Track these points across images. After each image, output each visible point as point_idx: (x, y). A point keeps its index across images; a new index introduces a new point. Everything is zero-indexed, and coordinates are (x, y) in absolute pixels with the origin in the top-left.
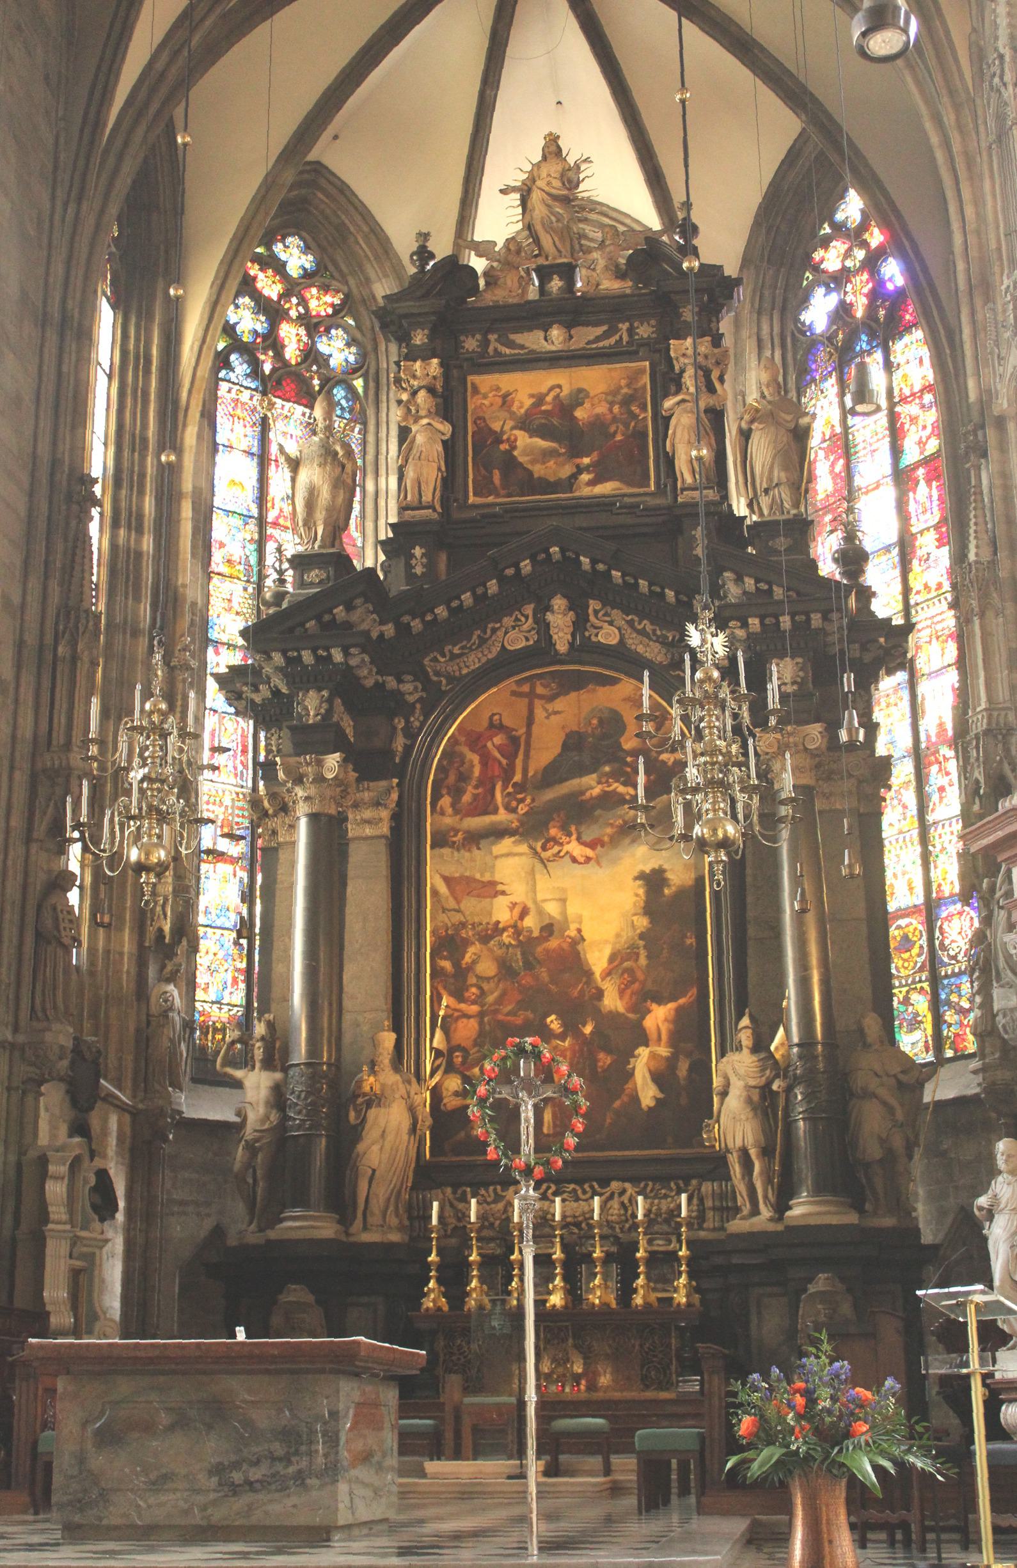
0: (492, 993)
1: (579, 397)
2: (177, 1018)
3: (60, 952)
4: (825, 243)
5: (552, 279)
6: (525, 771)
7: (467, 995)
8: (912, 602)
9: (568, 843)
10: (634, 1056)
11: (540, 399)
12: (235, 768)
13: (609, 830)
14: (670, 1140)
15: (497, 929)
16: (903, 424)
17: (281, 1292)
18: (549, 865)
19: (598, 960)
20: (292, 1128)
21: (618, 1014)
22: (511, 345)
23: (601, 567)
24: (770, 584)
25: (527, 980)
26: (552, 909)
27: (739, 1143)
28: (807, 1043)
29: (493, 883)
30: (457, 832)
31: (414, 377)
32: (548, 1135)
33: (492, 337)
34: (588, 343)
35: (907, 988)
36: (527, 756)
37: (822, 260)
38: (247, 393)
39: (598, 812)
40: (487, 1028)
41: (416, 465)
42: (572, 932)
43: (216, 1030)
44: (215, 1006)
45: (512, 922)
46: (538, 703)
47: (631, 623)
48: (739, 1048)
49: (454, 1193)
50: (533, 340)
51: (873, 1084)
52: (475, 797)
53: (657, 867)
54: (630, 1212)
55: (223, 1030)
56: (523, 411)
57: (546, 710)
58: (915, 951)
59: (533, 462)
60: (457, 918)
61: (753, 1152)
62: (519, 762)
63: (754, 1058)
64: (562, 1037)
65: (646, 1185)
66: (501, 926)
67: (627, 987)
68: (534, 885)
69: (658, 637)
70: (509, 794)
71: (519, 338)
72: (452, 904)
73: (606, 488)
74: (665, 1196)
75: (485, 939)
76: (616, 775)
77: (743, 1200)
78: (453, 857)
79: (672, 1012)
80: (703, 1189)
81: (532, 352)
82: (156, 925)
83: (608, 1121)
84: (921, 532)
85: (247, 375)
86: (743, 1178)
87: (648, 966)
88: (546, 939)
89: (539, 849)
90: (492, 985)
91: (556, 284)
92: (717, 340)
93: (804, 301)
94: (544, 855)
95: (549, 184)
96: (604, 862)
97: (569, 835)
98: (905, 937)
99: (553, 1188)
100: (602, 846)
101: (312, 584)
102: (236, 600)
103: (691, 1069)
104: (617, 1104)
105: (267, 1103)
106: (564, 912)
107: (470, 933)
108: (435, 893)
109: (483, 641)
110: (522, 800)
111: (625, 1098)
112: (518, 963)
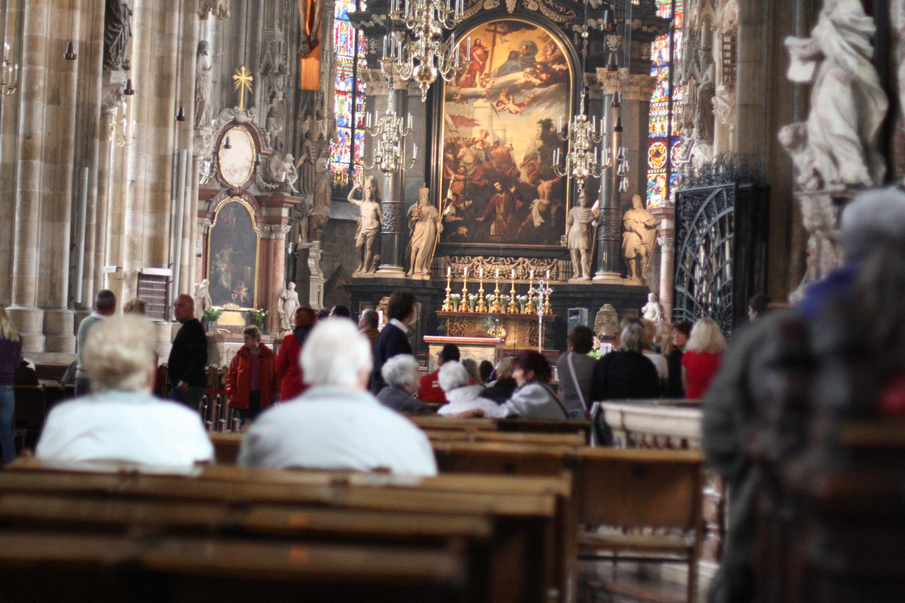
0: (471, 170)
2: (328, 175)
3: (310, 165)
7: (459, 171)
9: (509, 104)
10: (532, 203)
12: (347, 47)
13: (527, 99)
14: (546, 241)
15: (474, 142)
17: (380, 300)
18: (499, 113)
19: (519, 159)
24: (609, 3)
25: (487, 166)
26: (499, 134)
27: (576, 247)
28: (607, 209)
29: (473, 120)
30: (457, 94)
32: (493, 236)
35: (656, 175)
39: (523, 90)
40: (468, 186)
42: (508, 145)
43: (337, 175)
45: (481, 139)
46: (498, 36)
48: (579, 205)
49: (451, 258)
51: (634, 226)
52: (467, 79)
53: (548, 118)
54: (526, 271)
55: (340, 175)
57: (501, 39)
58: (661, 158)
60: (456, 135)
61: (582, 251)
63: (586, 210)
64: (501, 192)
65: (534, 260)
66: (476, 140)
67: (532, 171)
68: (492, 122)
69: (556, 9)
70: (482, 79)
72: (454, 128)
74: (542, 265)
75: (468, 146)
76: (532, 73)
77: (576, 269)
78: (455, 106)
79: (550, 185)
80: (559, 263)
82: (319, 131)
83: (519, 231)
86: (577, 261)
87: (541, 163)
88: (496, 148)
89: (495, 105)
90: (471, 166)
94: (497, 108)
96: (524, 114)
99: (494, 259)
100: (524, 106)
103: (557, 211)
104: (523, 224)
105: (372, 217)
106: (505, 136)
107: (462, 142)
108: (446, 123)
110: (487, 82)
111: (527, 221)
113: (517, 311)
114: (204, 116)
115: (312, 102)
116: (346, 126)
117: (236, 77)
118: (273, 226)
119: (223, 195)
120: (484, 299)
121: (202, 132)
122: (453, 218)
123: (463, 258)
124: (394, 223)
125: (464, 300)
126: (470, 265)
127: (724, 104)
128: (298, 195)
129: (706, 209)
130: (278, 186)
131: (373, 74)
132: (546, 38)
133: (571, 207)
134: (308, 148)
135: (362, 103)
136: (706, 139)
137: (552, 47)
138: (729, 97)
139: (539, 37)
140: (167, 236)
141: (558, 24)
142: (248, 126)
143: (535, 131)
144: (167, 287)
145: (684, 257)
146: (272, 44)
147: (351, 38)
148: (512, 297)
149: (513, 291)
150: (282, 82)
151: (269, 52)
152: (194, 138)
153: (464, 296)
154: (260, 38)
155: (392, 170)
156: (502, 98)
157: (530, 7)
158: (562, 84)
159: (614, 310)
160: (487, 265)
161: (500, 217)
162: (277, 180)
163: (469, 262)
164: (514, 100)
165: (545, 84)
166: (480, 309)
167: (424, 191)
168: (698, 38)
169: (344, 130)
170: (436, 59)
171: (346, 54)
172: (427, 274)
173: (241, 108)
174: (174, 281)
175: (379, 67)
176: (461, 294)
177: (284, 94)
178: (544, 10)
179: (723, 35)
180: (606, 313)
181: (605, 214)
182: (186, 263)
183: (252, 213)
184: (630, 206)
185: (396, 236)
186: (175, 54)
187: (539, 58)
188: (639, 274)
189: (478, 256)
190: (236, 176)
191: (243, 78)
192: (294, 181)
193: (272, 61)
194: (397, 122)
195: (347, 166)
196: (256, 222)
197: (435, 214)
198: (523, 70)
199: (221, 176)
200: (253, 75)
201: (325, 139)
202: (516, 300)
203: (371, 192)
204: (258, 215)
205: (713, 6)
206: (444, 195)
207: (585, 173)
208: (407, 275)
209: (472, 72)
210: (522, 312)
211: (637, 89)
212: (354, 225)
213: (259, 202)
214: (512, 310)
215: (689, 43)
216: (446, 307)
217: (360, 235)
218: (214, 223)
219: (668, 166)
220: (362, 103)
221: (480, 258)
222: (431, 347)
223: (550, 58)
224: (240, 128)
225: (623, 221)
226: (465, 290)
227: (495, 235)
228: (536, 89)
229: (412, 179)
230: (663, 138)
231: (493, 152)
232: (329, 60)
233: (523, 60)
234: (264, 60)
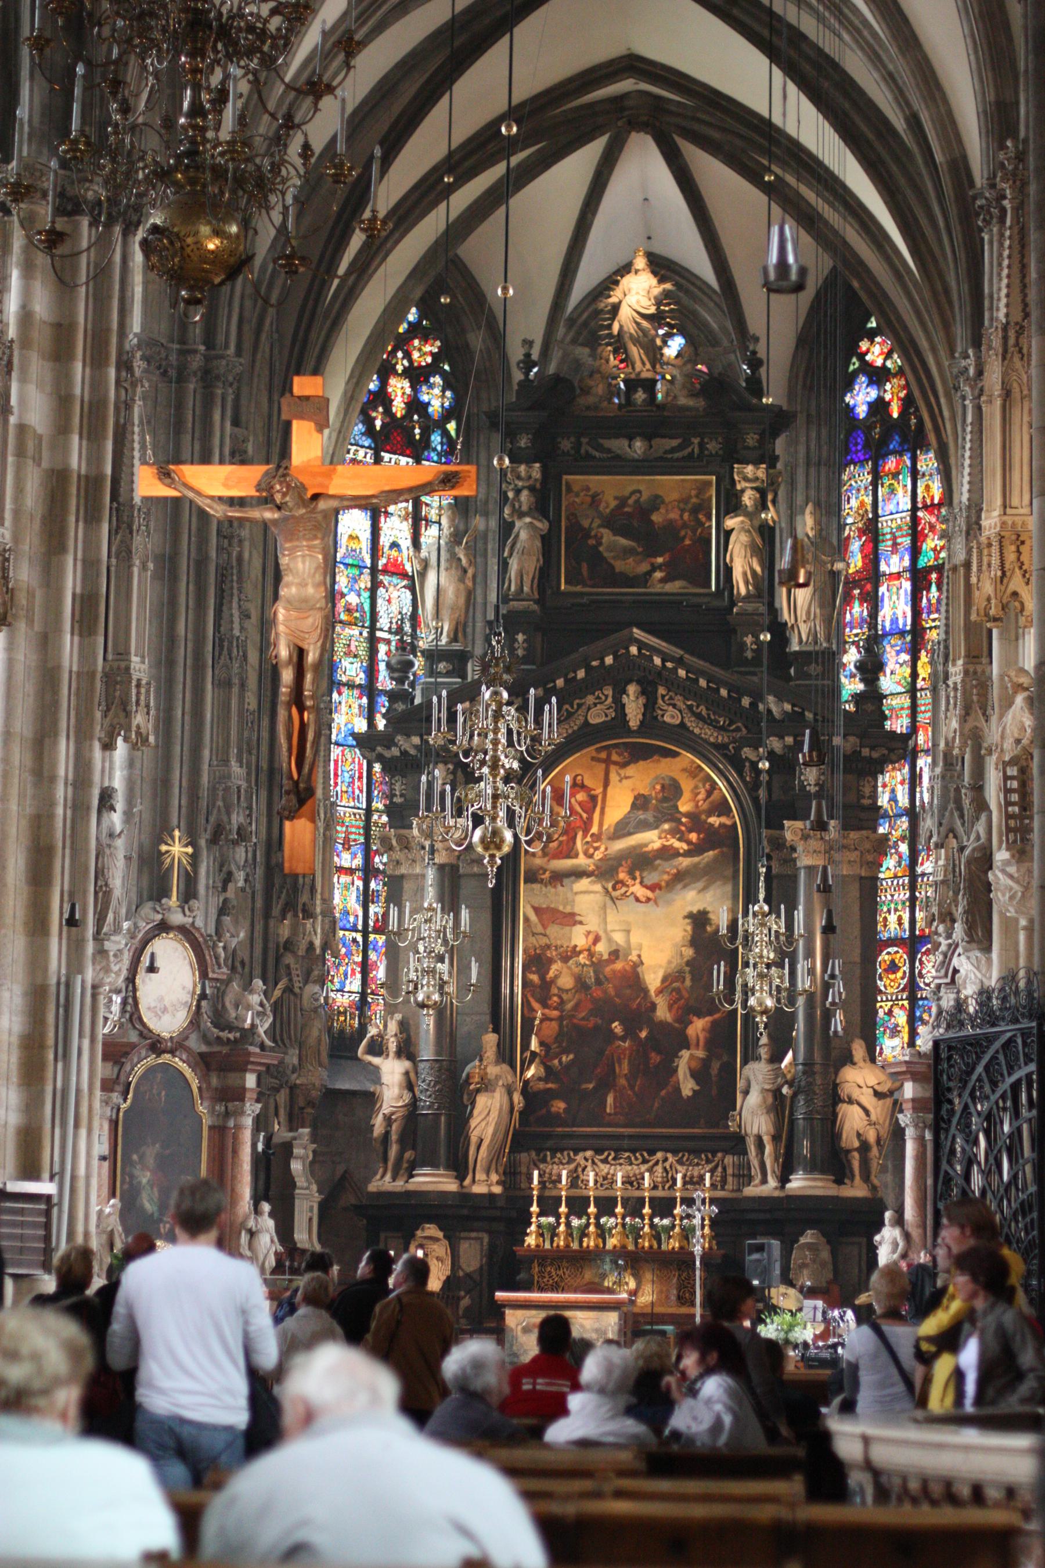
1: (656, 502)
3: (292, 997)
4: (871, 335)
5: (636, 391)
6: (601, 825)
8: (919, 686)
11: (623, 501)
13: (666, 877)
14: (702, 1121)
15: (575, 952)
16: (923, 529)
19: (653, 980)
20: (423, 1108)
21: (669, 1024)
22: (600, 448)
23: (669, 665)
25: (598, 993)
26: (619, 938)
27: (755, 1131)
28: (808, 1064)
29: (573, 915)
30: (545, 871)
31: (519, 478)
33: (584, 440)
34: (666, 452)
36: (602, 813)
37: (868, 351)
38: (362, 452)
39: (658, 862)
41: (520, 559)
42: (635, 958)
43: (339, 1013)
44: (339, 994)
46: (613, 769)
47: (690, 707)
48: (758, 1058)
49: (538, 1155)
50: (619, 445)
51: (856, 1094)
55: (345, 1012)
56: (608, 511)
58: (900, 974)
59: (614, 558)
60: (544, 941)
61: (766, 1139)
62: (596, 816)
63: (770, 1067)
64: (623, 1039)
67: (675, 1002)
68: (605, 919)
71: (607, 443)
72: (539, 929)
73: (675, 587)
74: (698, 1164)
75: (565, 959)
76: (673, 832)
77: (756, 1171)
80: (726, 1161)
81: (618, 457)
84: (931, 628)
85: (363, 434)
91: (640, 396)
92: (771, 461)
93: (849, 385)
94: (615, 894)
95: (638, 302)
96: (660, 902)
97: (634, 879)
98: (893, 961)
99: (613, 1154)
100: (660, 889)
101: (440, 674)
102: (354, 644)
103: (722, 1068)
104: (663, 1093)
105: (400, 1085)
106: (628, 941)
108: (527, 920)
109: (570, 715)
110: (597, 849)
111: (670, 1088)
112: (591, 980)
113: (655, 1246)
114: (110, 916)
115: (295, 889)
116: (357, 931)
117: (164, 848)
118: (230, 1105)
119: (143, 1053)
120: (598, 1225)
121: (107, 945)
122: (541, 1085)
123: (559, 1155)
124: (439, 1095)
125: (562, 1228)
126: (572, 1166)
127: (1010, 882)
128: (272, 1049)
129: (987, 1068)
130: (238, 1035)
131: (400, 838)
132: (694, 772)
133: (745, 1062)
134: (288, 967)
135: (380, 888)
136: (979, 942)
137: (707, 786)
138: (1018, 871)
139: (684, 770)
140: (48, 1126)
141: (717, 746)
142: (186, 933)
143: (679, 932)
144: (48, 1213)
145: (953, 1152)
146: (227, 789)
147: (360, 778)
148: (646, 1221)
149: (647, 1210)
150: (243, 855)
151: (220, 803)
152: (94, 955)
153: (563, 1220)
154: (205, 779)
155: (436, 1003)
156: (622, 876)
157: (667, 719)
158: (725, 849)
159: (823, 1240)
160: (602, 1166)
161: (623, 1082)
162: (236, 1023)
163: (570, 1161)
164: (642, 878)
165: (695, 850)
166: (590, 1242)
167: (490, 1039)
168: (958, 768)
169: (350, 935)
170: (511, 815)
171: (352, 804)
172: (498, 1183)
173: (173, 901)
174: (60, 1204)
175: (410, 827)
176: (558, 1217)
177: (247, 875)
178: (691, 723)
179: (1006, 764)
180: (809, 1246)
181: (804, 1073)
182: (82, 1171)
183: (195, 1083)
184: (848, 1059)
185: (443, 1119)
186: (60, 811)
187: (684, 806)
188: (866, 1177)
189: (585, 1150)
190: (166, 1018)
191: (177, 849)
192: (267, 1025)
193: (225, 818)
194: (442, 920)
195: (356, 997)
196: (201, 1098)
197: (510, 1079)
198: (656, 828)
199: (140, 1019)
200: (192, 843)
201: (318, 951)
202: (652, 1226)
203: (399, 1042)
204: (204, 1086)
205: (984, 714)
206: (526, 1044)
207: (770, 1003)
208: (461, 1186)
209: (570, 833)
210: (664, 1247)
211: (854, 856)
212: (371, 1099)
213: (204, 1063)
214: (647, 1244)
215: (943, 777)
216: (531, 1241)
217: (380, 1117)
218: (129, 1101)
219: (912, 987)
220: (380, 888)
221: (589, 1153)
222: (508, 1312)
223: (704, 806)
224: (171, 935)
225: (836, 1085)
226: (563, 1209)
227: (616, 1114)
228: (681, 859)
229: (468, 1019)
230: (902, 939)
231: (608, 970)
232: (322, 815)
233: (657, 809)
234: (212, 819)
